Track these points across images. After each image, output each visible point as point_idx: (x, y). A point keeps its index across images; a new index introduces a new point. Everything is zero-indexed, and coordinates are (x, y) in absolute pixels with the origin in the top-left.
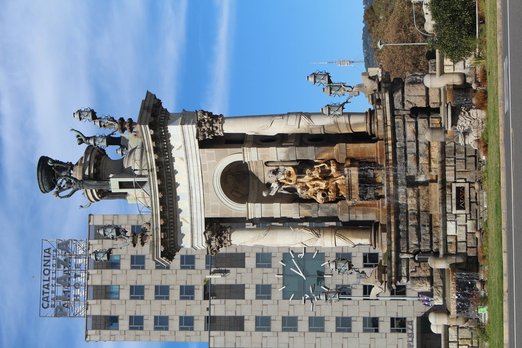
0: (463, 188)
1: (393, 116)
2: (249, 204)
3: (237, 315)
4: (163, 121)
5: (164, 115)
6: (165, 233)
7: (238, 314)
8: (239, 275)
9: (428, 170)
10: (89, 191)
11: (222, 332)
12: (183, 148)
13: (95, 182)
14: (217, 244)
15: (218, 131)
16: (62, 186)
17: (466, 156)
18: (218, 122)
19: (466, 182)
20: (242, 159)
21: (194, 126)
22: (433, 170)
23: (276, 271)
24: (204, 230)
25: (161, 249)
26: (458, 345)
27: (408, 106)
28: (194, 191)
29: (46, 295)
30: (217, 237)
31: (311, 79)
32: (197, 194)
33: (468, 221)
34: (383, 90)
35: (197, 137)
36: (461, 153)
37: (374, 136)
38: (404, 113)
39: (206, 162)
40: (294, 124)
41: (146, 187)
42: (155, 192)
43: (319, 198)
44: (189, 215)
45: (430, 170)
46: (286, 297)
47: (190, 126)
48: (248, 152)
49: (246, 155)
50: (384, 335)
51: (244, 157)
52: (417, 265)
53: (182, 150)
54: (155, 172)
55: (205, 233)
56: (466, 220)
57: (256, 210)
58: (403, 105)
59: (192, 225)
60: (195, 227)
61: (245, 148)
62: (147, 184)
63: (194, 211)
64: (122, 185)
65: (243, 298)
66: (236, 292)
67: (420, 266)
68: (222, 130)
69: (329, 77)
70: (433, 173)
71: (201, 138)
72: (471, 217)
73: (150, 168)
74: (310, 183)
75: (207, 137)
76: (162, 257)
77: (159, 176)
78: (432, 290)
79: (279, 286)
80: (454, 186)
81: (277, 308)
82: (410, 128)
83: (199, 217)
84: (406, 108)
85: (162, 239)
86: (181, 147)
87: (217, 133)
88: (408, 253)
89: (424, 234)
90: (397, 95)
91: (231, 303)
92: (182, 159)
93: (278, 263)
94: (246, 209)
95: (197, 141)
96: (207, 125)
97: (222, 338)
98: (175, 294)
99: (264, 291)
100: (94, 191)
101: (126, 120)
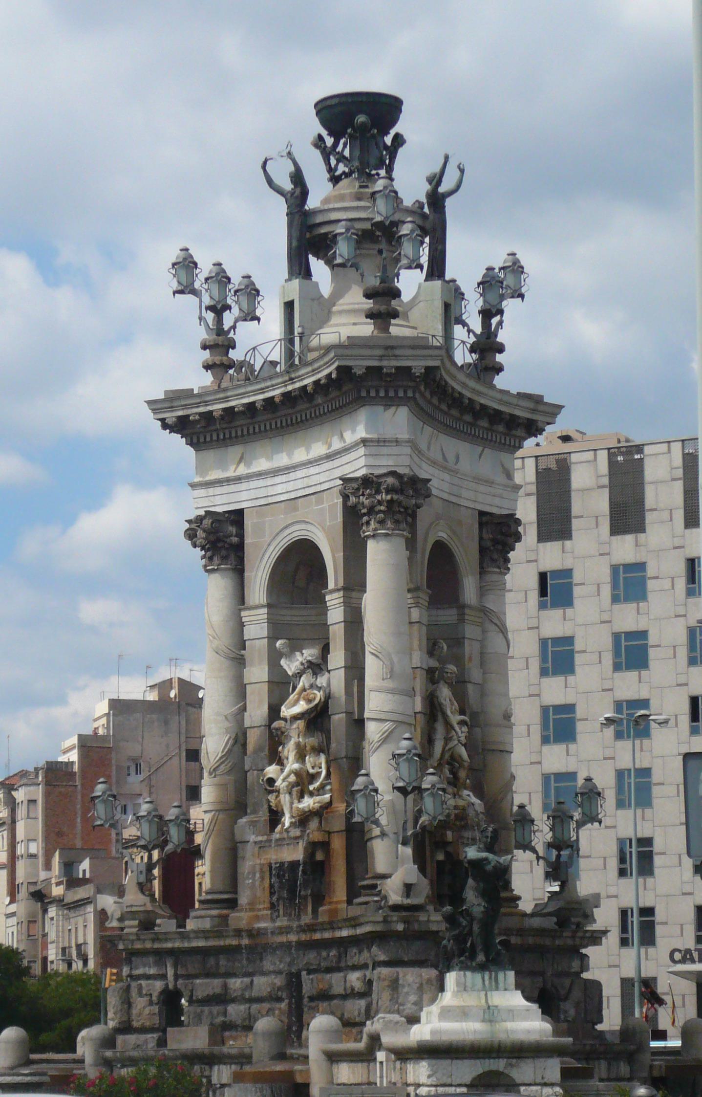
18: (377, 525)
20: (330, 588)
28: (283, 478)
54: (290, 388)
67: (151, 1003)
68: (374, 536)
83: (244, 496)
85: (188, 416)
88: (176, 977)
89: (211, 1012)
94: (257, 602)
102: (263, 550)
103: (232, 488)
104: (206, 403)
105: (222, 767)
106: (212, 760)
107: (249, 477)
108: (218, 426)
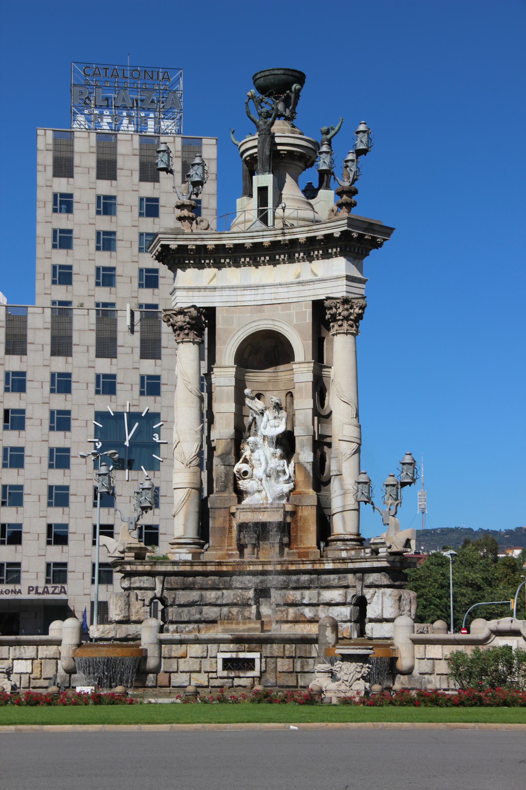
0: (252, 669)
1: (354, 571)
2: (234, 369)
3: (74, 347)
4: (352, 250)
5: (360, 252)
6: (195, 251)
7: (74, 348)
8: (129, 350)
9: (278, 619)
10: (255, 143)
11: (49, 326)
12: (314, 278)
13: (268, 153)
14: (179, 324)
15: (336, 327)
16: (263, 104)
17: (297, 672)
19: (261, 672)
20: (297, 360)
21: (344, 294)
22: (278, 626)
23: (135, 403)
24: (198, 305)
25: (173, 245)
26: (33, 659)
27: (368, 593)
28: (253, 292)
29: (103, 73)
30: (189, 323)
31: (408, 459)
32: (249, 298)
33: (207, 674)
34: (392, 558)
35: (328, 298)
36: (302, 666)
37: (327, 545)
38: (359, 588)
39: (293, 310)
40: (345, 433)
41: (260, 225)
42: (253, 237)
43: (240, 466)
44: (220, 284)
45: (277, 622)
46: (100, 416)
47: (344, 288)
48: (306, 369)
49: (302, 365)
50: (42, 553)
51: (299, 363)
52: (147, 602)
53: (311, 277)
54: (280, 238)
55: (194, 306)
56: (209, 672)
57: (224, 378)
58: (369, 586)
59: (205, 288)
60: (202, 293)
61: (312, 365)
62: (264, 227)
63: (226, 292)
64: (263, 190)
65: (98, 356)
66: (106, 347)
69: (410, 484)
70: (274, 626)
71: (327, 303)
72: (212, 678)
73: (286, 231)
74: (261, 455)
75: (328, 312)
76: (162, 246)
77: (275, 244)
78: (111, 622)
79: (114, 406)
80: (256, 655)
81: (84, 404)
82: (335, 595)
83: (217, 299)
84: (365, 591)
85: (187, 246)
86: (315, 275)
87: (333, 326)
90: (384, 579)
91: (91, 339)
92: (298, 276)
93: (147, 405)
94: (227, 364)
95: (323, 297)
96: (345, 313)
97: (40, 325)
98: (104, 259)
99: (107, 385)
100: (255, 150)
101: (354, 198)
102: (234, 333)
103: (208, 293)
104: (203, 239)
105: (194, 462)
106: (187, 458)
107: (223, 288)
108: (203, 256)
